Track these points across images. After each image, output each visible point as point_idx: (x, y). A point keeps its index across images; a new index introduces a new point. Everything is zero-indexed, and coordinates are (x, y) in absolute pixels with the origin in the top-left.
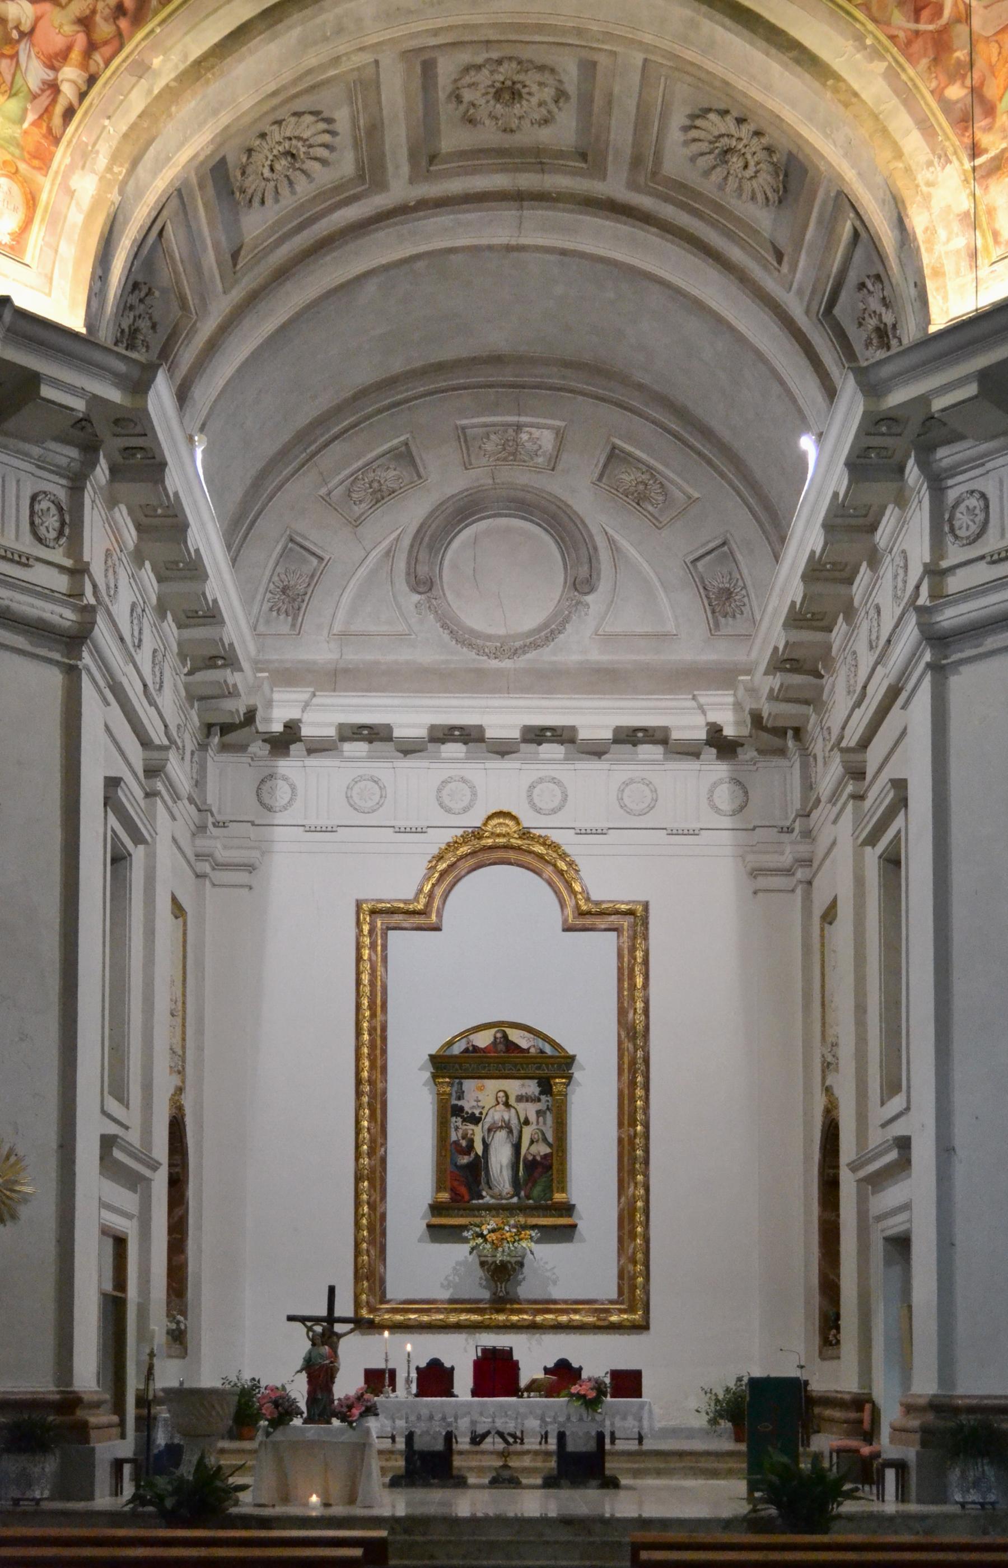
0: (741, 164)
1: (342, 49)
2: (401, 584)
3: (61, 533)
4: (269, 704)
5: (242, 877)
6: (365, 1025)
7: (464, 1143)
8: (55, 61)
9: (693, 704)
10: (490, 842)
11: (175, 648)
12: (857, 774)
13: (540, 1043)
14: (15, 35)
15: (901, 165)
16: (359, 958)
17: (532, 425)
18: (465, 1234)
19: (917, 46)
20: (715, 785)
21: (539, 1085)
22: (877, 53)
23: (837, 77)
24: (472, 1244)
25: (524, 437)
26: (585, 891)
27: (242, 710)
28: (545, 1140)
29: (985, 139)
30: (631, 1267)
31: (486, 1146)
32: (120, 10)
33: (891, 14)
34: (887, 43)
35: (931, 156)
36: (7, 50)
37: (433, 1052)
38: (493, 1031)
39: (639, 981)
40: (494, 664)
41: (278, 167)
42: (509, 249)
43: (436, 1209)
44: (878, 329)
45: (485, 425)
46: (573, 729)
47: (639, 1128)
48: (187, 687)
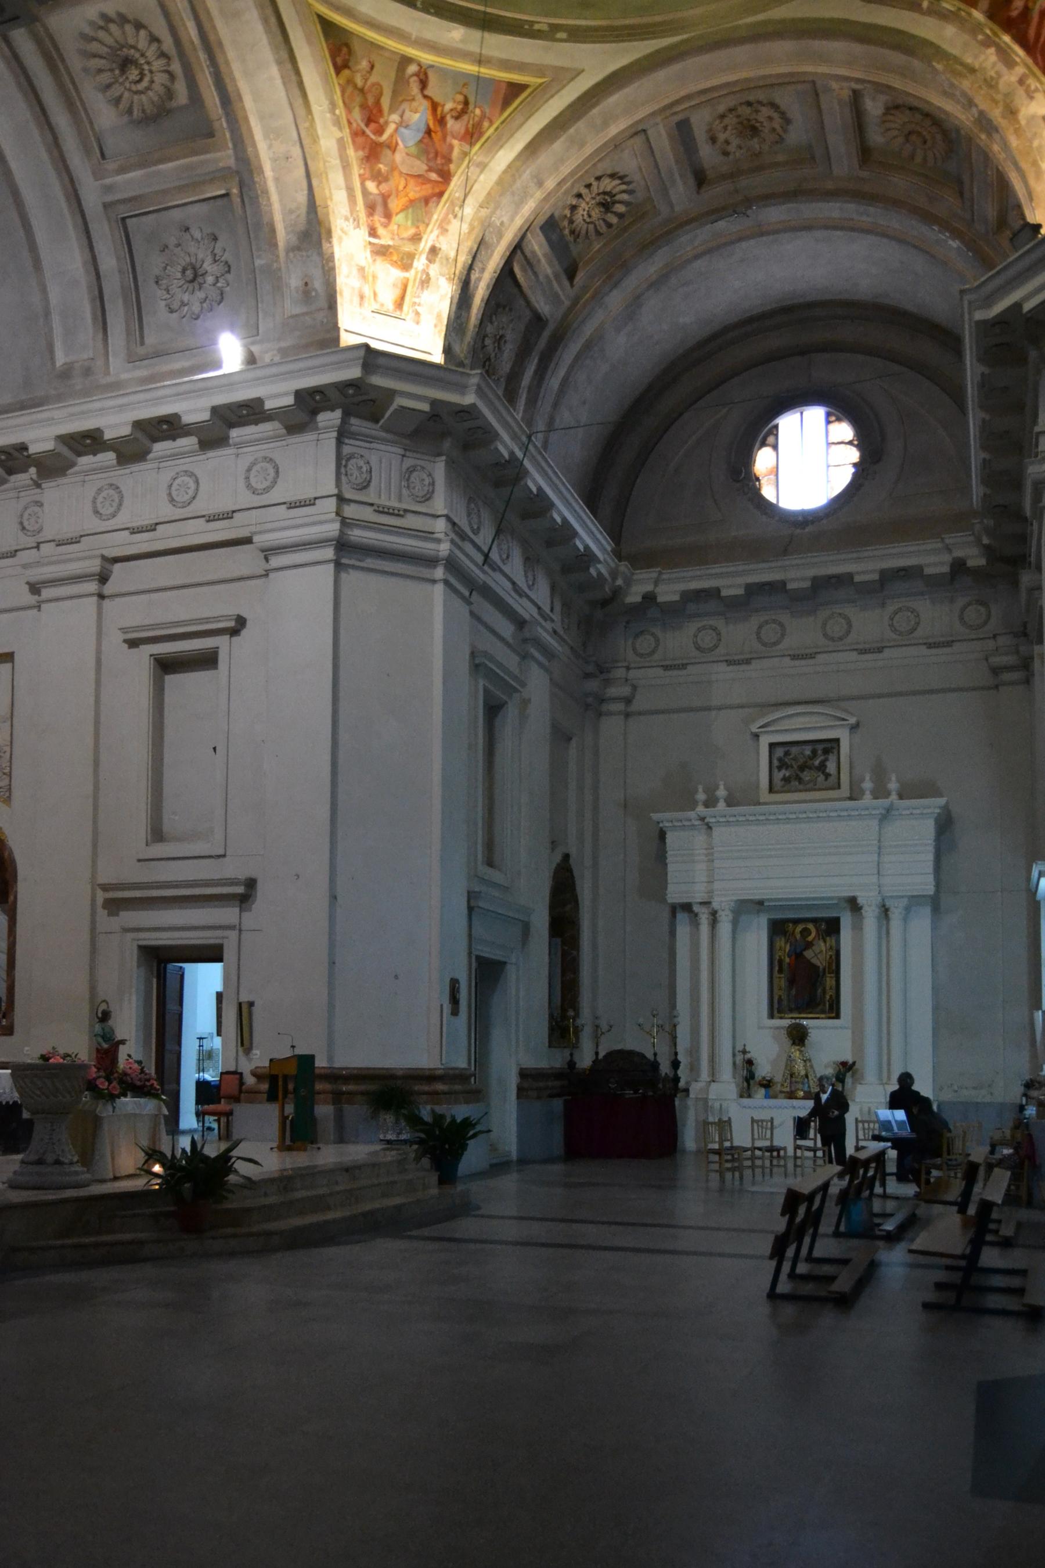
19: (360, 140)
22: (337, 123)
29: (381, 231)
33: (354, 107)
34: (345, 122)
35: (349, 214)
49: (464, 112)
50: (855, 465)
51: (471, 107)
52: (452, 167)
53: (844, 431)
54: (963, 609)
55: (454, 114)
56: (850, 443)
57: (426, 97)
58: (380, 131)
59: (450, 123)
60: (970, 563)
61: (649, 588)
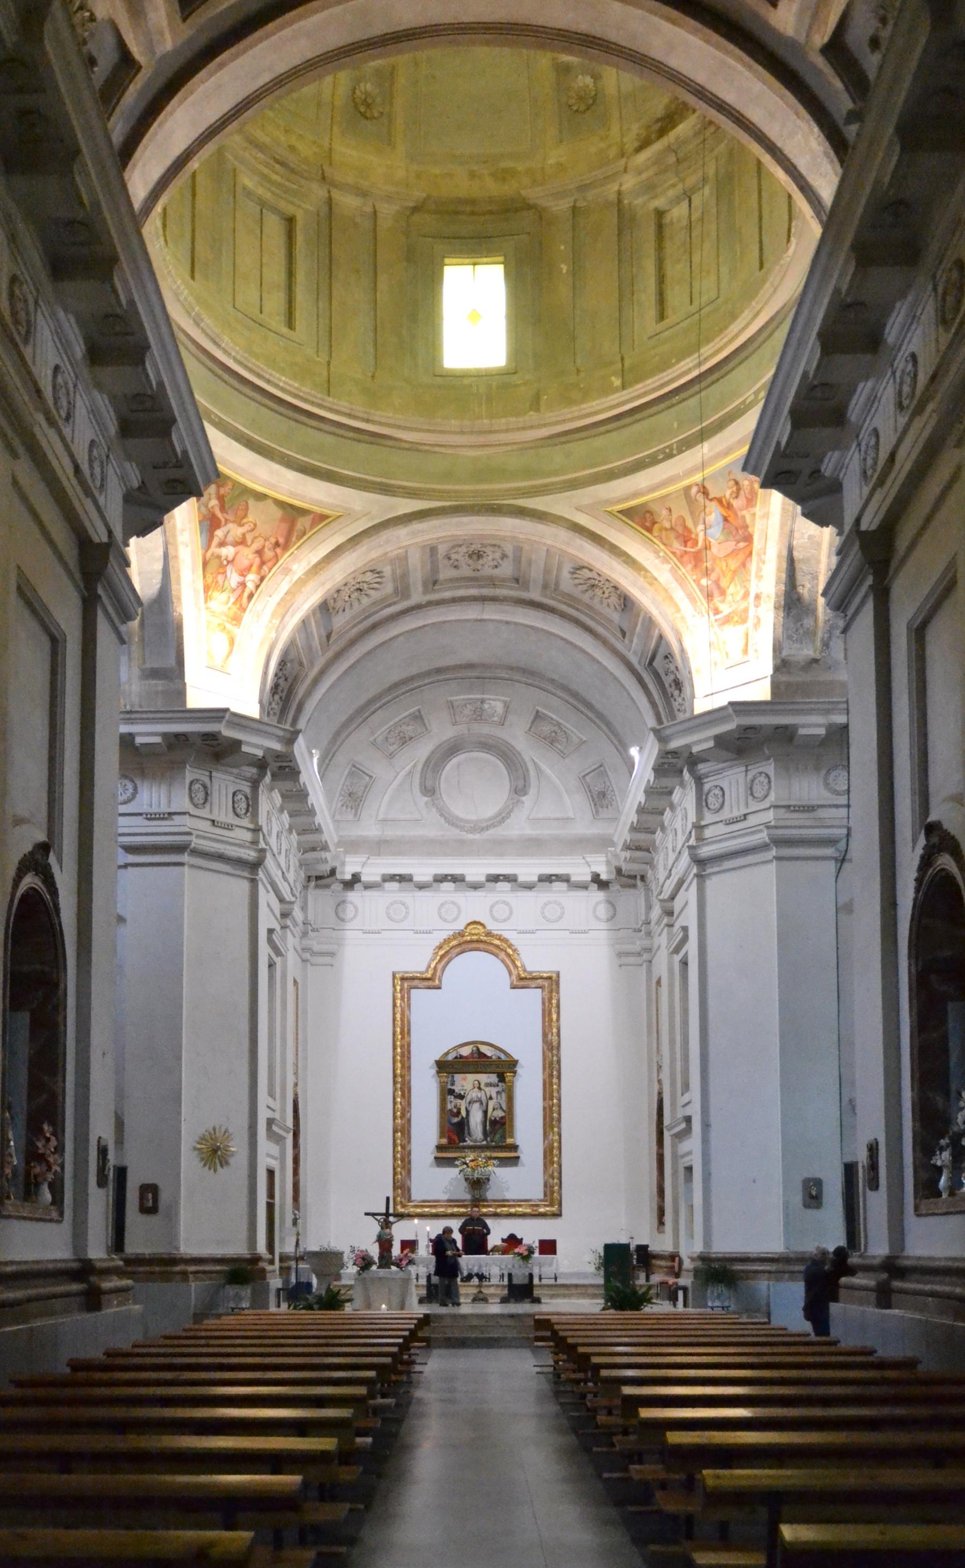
0: (601, 592)
1: (389, 549)
2: (417, 790)
3: (247, 811)
4: (343, 864)
5: (327, 960)
6: (398, 1043)
7: (455, 1110)
8: (243, 573)
9: (583, 861)
10: (469, 938)
11: (295, 844)
12: (670, 913)
13: (498, 1053)
14: (225, 563)
15: (679, 615)
16: (394, 1005)
17: (490, 699)
18: (457, 1163)
19: (686, 558)
20: (597, 904)
21: (498, 1077)
22: (665, 560)
23: (646, 570)
24: (461, 1168)
25: (486, 706)
26: (523, 966)
27: (329, 869)
28: (501, 1108)
29: (722, 607)
30: (551, 1180)
31: (468, 1112)
32: (277, 544)
34: (671, 555)
36: (221, 570)
37: (437, 1059)
38: (471, 1046)
39: (554, 1016)
40: (471, 836)
41: (352, 596)
42: (476, 620)
43: (440, 1148)
44: (675, 681)
45: (463, 700)
46: (515, 876)
47: (555, 1101)
48: (299, 861)
49: (739, 490)
51: (741, 483)
52: (750, 530)
55: (734, 495)
57: (711, 500)
59: (735, 503)
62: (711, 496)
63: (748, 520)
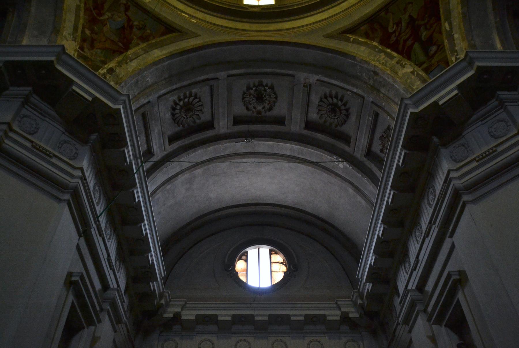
29: (86, 50)
50: (285, 273)
52: (130, 45)
53: (278, 258)
54: (345, 344)
56: (282, 263)
57: (126, 15)
58: (101, 15)
59: (135, 30)
60: (351, 315)
61: (179, 310)
62: (129, 13)
63: (134, 41)
